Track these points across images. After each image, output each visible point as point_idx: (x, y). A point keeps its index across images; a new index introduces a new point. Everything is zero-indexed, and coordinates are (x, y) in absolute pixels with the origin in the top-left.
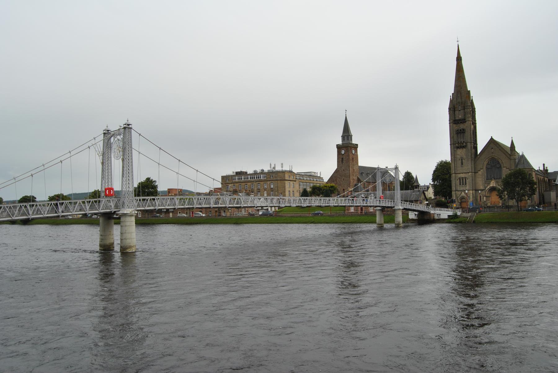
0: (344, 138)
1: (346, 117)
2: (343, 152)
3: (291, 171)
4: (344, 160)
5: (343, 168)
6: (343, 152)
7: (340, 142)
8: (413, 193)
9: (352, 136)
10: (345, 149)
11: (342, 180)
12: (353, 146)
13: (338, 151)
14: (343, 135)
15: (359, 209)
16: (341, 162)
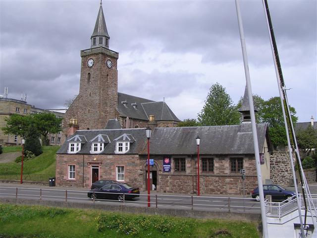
0: (95, 39)
1: (101, 7)
2: (90, 63)
3: (24, 102)
4: (92, 76)
5: (89, 91)
6: (90, 63)
7: (88, 45)
8: (239, 133)
9: (109, 38)
10: (94, 58)
11: (87, 111)
12: (108, 54)
13: (82, 62)
14: (94, 35)
15: (89, 173)
16: (86, 80)
